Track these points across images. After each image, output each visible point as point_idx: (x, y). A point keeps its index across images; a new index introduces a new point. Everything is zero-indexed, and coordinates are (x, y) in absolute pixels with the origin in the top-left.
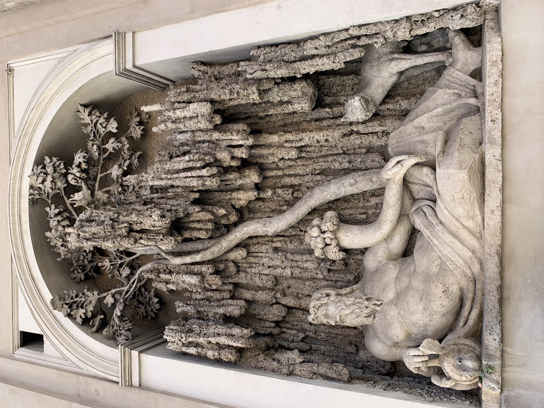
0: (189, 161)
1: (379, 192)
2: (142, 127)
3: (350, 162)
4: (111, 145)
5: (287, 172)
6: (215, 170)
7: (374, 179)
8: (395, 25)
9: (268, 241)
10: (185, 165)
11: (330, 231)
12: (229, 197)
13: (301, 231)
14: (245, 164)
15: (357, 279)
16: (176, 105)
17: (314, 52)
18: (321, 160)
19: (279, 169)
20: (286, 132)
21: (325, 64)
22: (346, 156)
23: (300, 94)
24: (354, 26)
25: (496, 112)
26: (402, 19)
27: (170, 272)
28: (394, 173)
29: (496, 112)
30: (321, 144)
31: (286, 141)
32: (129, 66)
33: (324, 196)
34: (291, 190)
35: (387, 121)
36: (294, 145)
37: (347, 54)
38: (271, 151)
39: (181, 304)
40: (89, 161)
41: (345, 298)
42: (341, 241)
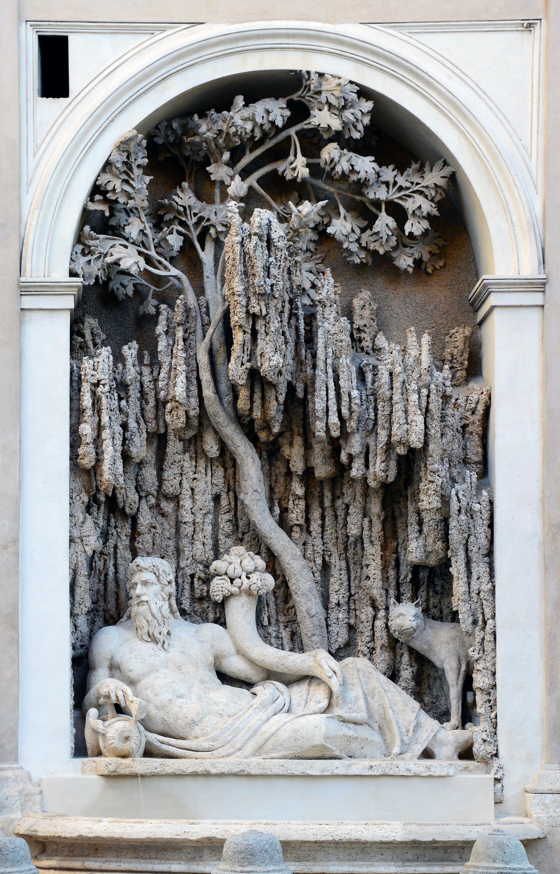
0: (349, 395)
1: (297, 644)
2: (410, 270)
3: (338, 604)
4: (385, 222)
5: (329, 513)
6: (335, 433)
7: (315, 638)
8: (490, 672)
9: (229, 484)
10: (344, 390)
11: (250, 586)
12: (296, 430)
13: (244, 534)
14: (342, 470)
15: (183, 613)
16: (425, 392)
17: (474, 576)
18: (343, 564)
19: (333, 501)
20: (384, 523)
21: (459, 587)
22: (346, 599)
23: (429, 549)
24: (495, 626)
25: (380, 770)
26: (495, 679)
27: (185, 340)
29: (380, 770)
30: (365, 569)
31: (371, 522)
33: (295, 575)
34: (302, 521)
35: (387, 654)
36: (366, 533)
37: (466, 616)
38: (359, 498)
39: (134, 352)
41: (167, 605)
42: (237, 598)
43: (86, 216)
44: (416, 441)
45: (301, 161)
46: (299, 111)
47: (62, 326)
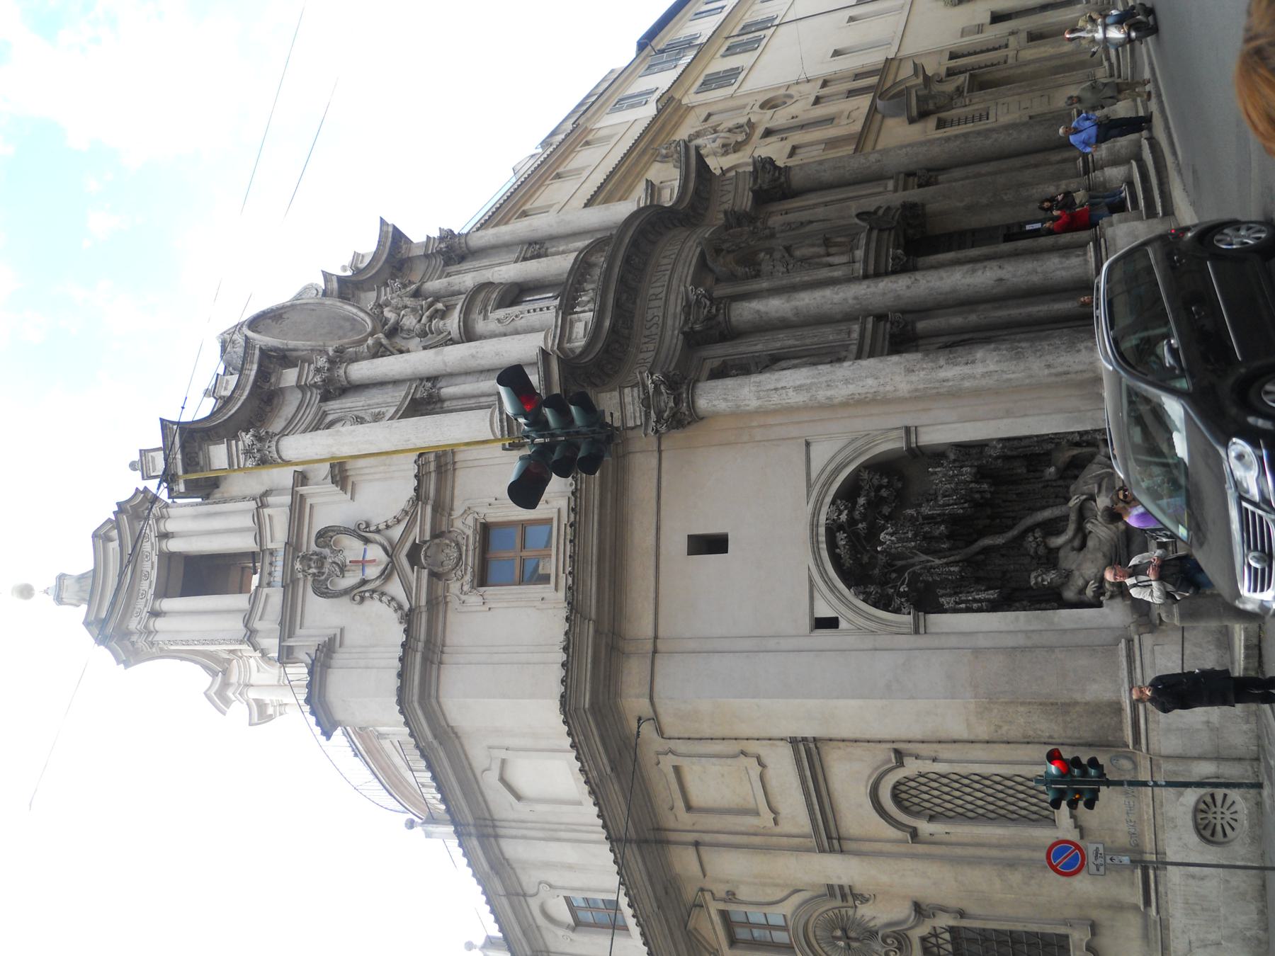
1: (1065, 518)
28: (1074, 502)
32: (914, 445)
40: (869, 502)
43: (886, 608)
44: (974, 470)
45: (860, 526)
46: (841, 527)
47: (934, 618)
